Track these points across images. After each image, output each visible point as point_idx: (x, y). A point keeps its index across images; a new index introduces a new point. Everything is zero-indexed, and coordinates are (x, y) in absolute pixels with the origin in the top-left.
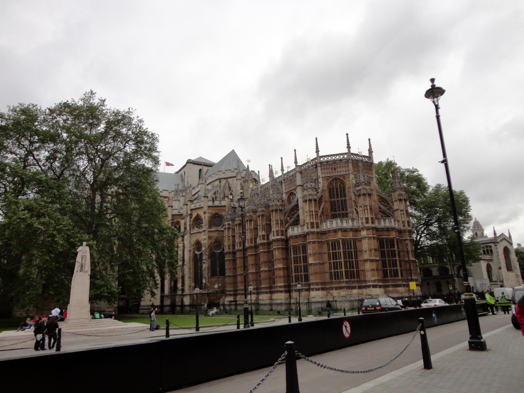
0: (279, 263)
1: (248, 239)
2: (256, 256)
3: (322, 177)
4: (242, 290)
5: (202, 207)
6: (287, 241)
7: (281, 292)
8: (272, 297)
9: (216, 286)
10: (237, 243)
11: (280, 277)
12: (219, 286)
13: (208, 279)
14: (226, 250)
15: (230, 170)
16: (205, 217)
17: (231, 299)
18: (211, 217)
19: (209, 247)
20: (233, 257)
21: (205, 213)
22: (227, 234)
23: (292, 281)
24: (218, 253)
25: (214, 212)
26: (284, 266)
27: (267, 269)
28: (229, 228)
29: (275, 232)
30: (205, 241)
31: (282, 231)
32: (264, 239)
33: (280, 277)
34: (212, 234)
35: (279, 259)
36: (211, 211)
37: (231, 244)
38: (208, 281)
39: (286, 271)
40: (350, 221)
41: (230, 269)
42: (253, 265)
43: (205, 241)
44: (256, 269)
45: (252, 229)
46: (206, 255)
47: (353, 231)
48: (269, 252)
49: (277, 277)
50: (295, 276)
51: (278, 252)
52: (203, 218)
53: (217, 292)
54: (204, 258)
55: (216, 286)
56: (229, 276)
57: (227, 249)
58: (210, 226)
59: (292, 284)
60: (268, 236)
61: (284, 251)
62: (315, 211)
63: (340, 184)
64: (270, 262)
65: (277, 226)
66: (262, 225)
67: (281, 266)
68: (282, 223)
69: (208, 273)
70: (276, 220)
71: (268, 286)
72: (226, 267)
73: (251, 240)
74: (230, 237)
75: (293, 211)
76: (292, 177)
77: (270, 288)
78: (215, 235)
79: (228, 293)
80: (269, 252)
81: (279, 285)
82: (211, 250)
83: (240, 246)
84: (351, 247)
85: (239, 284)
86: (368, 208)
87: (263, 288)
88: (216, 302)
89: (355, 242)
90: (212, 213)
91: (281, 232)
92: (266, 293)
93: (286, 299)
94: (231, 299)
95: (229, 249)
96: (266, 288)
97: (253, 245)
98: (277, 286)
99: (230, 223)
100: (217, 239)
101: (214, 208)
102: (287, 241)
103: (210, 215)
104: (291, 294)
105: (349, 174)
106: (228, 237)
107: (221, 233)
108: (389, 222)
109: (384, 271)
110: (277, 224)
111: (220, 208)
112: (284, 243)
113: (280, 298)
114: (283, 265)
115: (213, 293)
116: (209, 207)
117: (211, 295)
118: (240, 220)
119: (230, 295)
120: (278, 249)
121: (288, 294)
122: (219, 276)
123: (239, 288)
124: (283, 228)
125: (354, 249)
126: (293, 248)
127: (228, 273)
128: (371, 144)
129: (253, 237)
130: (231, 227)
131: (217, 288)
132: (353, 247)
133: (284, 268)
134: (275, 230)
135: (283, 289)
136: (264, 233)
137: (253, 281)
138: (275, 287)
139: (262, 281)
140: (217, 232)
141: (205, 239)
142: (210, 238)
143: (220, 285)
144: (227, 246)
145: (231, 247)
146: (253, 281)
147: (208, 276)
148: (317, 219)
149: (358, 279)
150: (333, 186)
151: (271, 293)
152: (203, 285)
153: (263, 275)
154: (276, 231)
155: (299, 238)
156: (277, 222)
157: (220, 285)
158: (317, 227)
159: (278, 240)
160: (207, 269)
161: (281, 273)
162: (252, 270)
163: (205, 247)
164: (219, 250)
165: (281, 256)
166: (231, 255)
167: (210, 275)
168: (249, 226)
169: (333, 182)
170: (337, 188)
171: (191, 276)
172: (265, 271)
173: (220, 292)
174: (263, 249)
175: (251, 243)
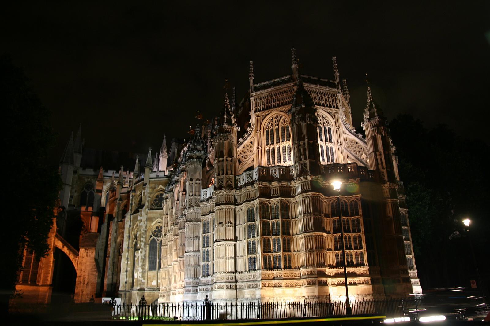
38: (143, 277)
131: (154, 286)
141: (141, 221)
147: (143, 269)
152: (135, 281)
167: (146, 267)
171: (129, 269)
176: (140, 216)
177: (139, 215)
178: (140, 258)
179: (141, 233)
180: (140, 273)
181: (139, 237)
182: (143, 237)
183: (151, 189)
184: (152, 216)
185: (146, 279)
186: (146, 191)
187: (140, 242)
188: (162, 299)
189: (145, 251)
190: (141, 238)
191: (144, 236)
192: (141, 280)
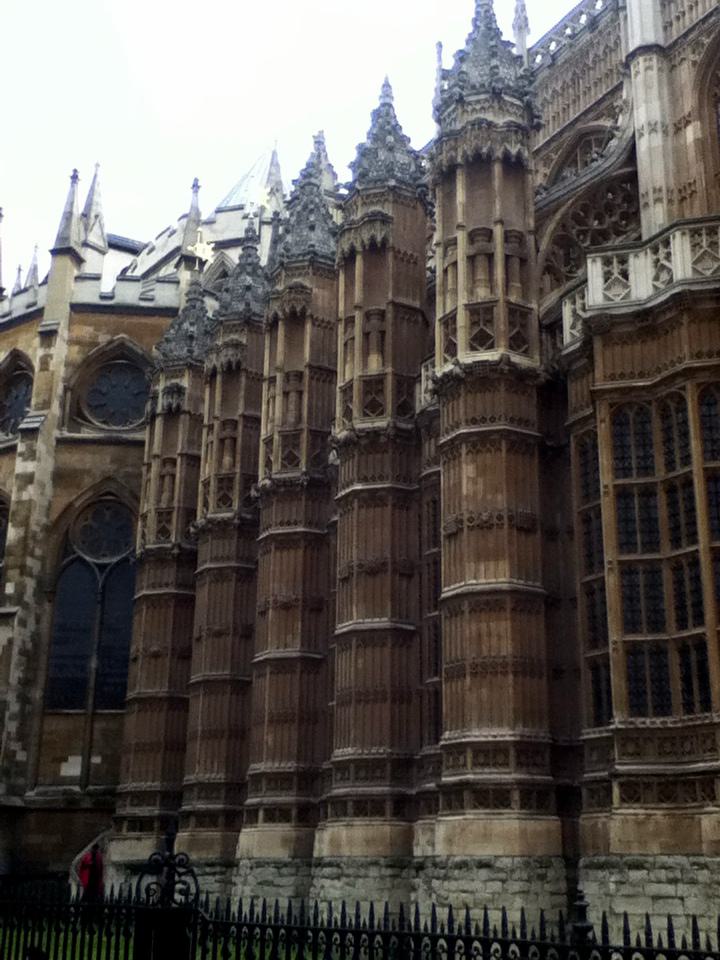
0: (481, 556)
1: (269, 442)
2: (318, 544)
4: (207, 790)
5: (40, 313)
6: (551, 391)
7: (491, 798)
8: (408, 839)
9: (72, 768)
10: (206, 484)
11: (485, 670)
12: (87, 766)
13: (23, 717)
14: (145, 537)
15: (241, 208)
16: (45, 362)
17: (142, 848)
18: (87, 363)
19: (48, 529)
20: (179, 586)
21: (48, 336)
22: (156, 450)
23: (586, 709)
24: (102, 567)
25: (103, 339)
26: (520, 584)
27: (382, 622)
28: (172, 414)
29: (462, 319)
30: (30, 492)
31: (518, 314)
32: (373, 408)
33: (485, 670)
34: (74, 459)
35: (485, 527)
36: (85, 331)
37: (176, 504)
39: (536, 627)
41: (156, 656)
42: (286, 607)
43: (30, 492)
44: (308, 641)
45: (300, 375)
46: (24, 570)
48: (403, 500)
49: (458, 673)
50: (633, 651)
51: (482, 471)
52: (36, 364)
53: (71, 805)
54: (10, 589)
55: (72, 768)
56: (145, 702)
57: (151, 537)
58: (74, 415)
59: (590, 734)
60: (406, 385)
61: (532, 469)
64: (406, 572)
65: (481, 275)
66: (368, 316)
67: (494, 576)
68: (518, 260)
69: (26, 683)
70: (472, 237)
71: (381, 751)
72: (137, 646)
73: (290, 439)
74: (173, 462)
75: (600, 218)
76: (588, 36)
77: (403, 767)
78: (96, 463)
79: (130, 810)
80: (403, 500)
81: (479, 734)
82: (65, 548)
83: (224, 501)
85: (196, 749)
87: (342, 766)
88: (54, 868)
90: (95, 344)
91: (512, 324)
92: (365, 807)
93: (536, 867)
94: (142, 848)
95: (163, 532)
96: (366, 769)
97: (297, 474)
98: (459, 749)
99: (185, 382)
100: (112, 487)
101: (105, 318)
102: (551, 391)
103: (76, 353)
104: (585, 821)
106: (165, 462)
107: (133, 452)
110: (481, 262)
111: (135, 320)
112: (529, 407)
113: (484, 852)
114: (518, 570)
115: (47, 811)
116: (77, 308)
117: (32, 818)
118: (237, 345)
119: (141, 825)
120: (479, 443)
121: (547, 825)
122: (95, 707)
123: (190, 778)
124: (525, 295)
126: (618, 420)
127: (143, 683)
129: (304, 425)
130: (186, 407)
131: (71, 780)
133: (520, 601)
134: (463, 300)
135: (508, 776)
136: (375, 365)
137: (278, 720)
138: (437, 765)
139: (346, 715)
140: (111, 449)
141: (28, 479)
142: (60, 477)
143: (96, 760)
144: (152, 518)
145: (174, 526)
146: (278, 720)
147: (23, 699)
151: (408, 808)
153: (348, 669)
154: (473, 309)
155: (675, 323)
156: (481, 244)
157: (96, 760)
159: (478, 378)
160: (15, 657)
161: (500, 637)
162: (277, 645)
163: (25, 523)
164: (113, 554)
165: (501, 501)
166: (170, 574)
167: (37, 694)
168: (280, 357)
172: (367, 638)
173: (87, 804)
174: (365, 480)
175: (290, 460)
176: (25, 460)
177: (21, 454)
178: (16, 650)
179: (26, 532)
180: (10, 719)
181: (18, 551)
182: (32, 555)
183: (76, 348)
184: (79, 466)
185: (34, 749)
186: (53, 351)
187: (22, 574)
188: (134, 842)
189: (38, 621)
190: (24, 555)
191: (38, 552)
192: (14, 752)
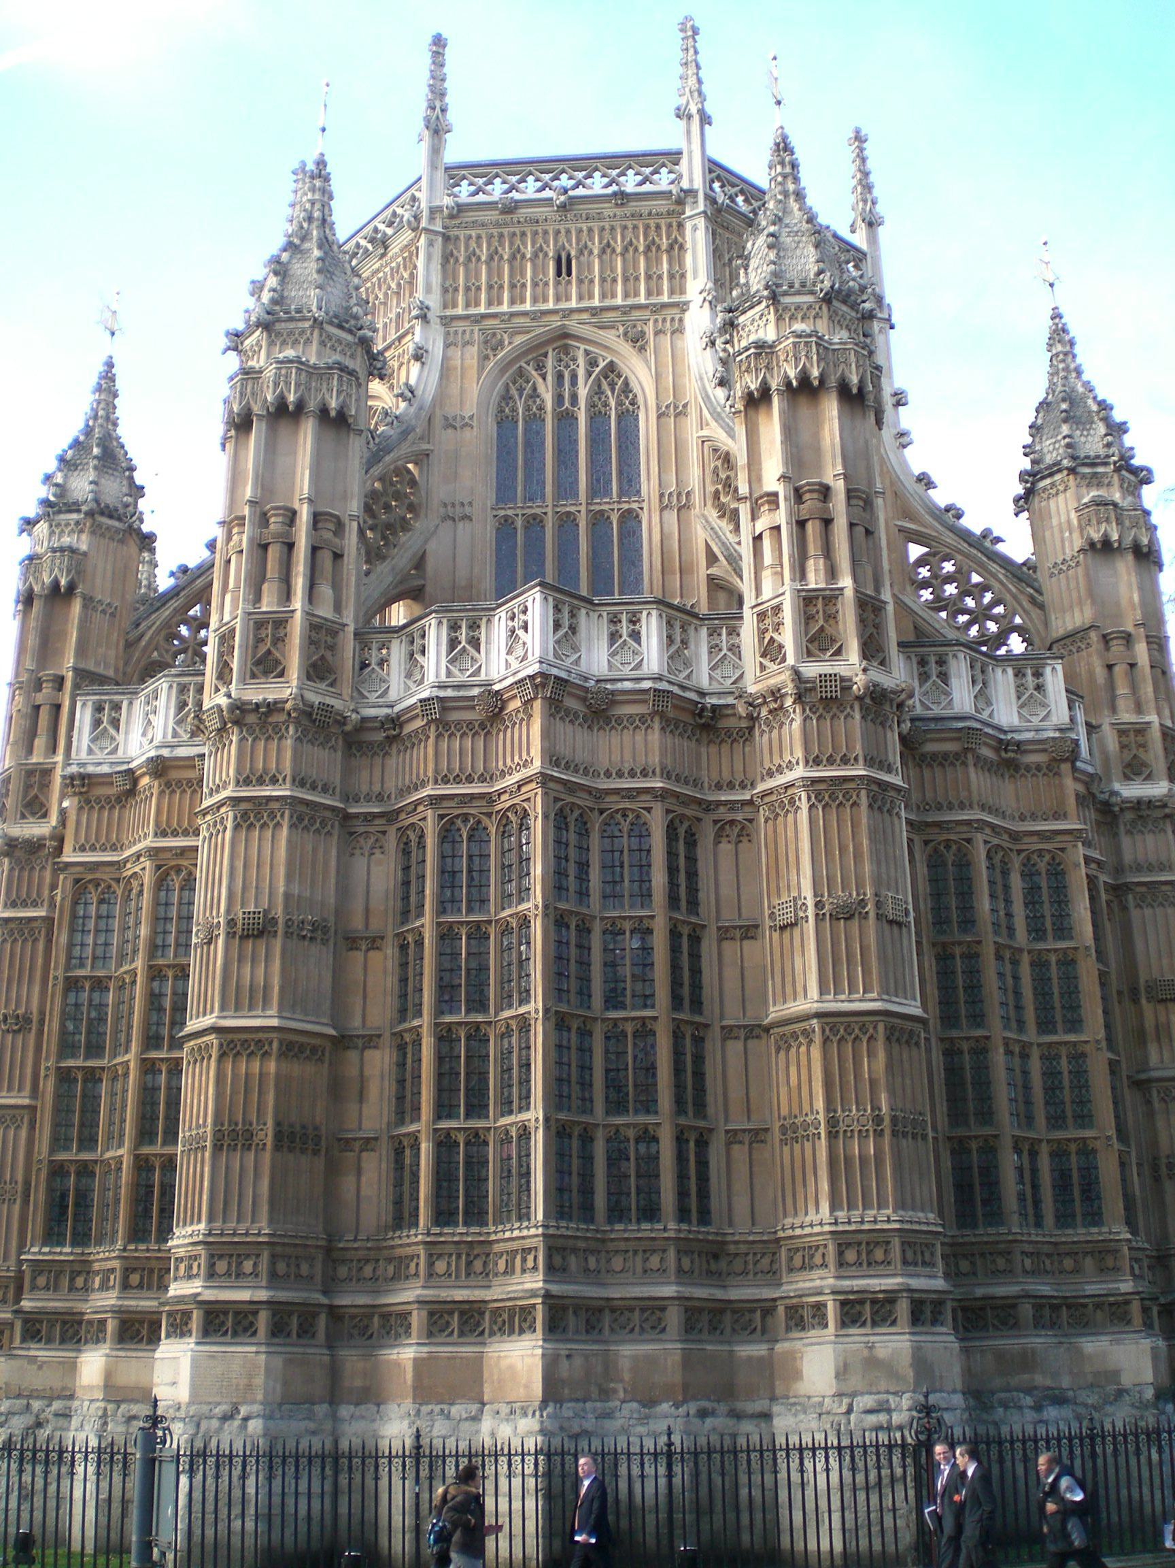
3: (446, 321)
40: (652, 628)
47: (670, 725)
62: (316, 518)
63: (597, 391)
84: (644, 880)
86: (839, 506)
89: (691, 843)
105: (683, 307)
108: (1020, 689)
109: (959, 1148)
125: (673, 900)
128: (870, 165)
132: (659, 878)
148: (326, 591)
149: (693, 1229)
150: (535, 394)
158: (318, 670)
169: (540, 367)
170: (566, 419)
